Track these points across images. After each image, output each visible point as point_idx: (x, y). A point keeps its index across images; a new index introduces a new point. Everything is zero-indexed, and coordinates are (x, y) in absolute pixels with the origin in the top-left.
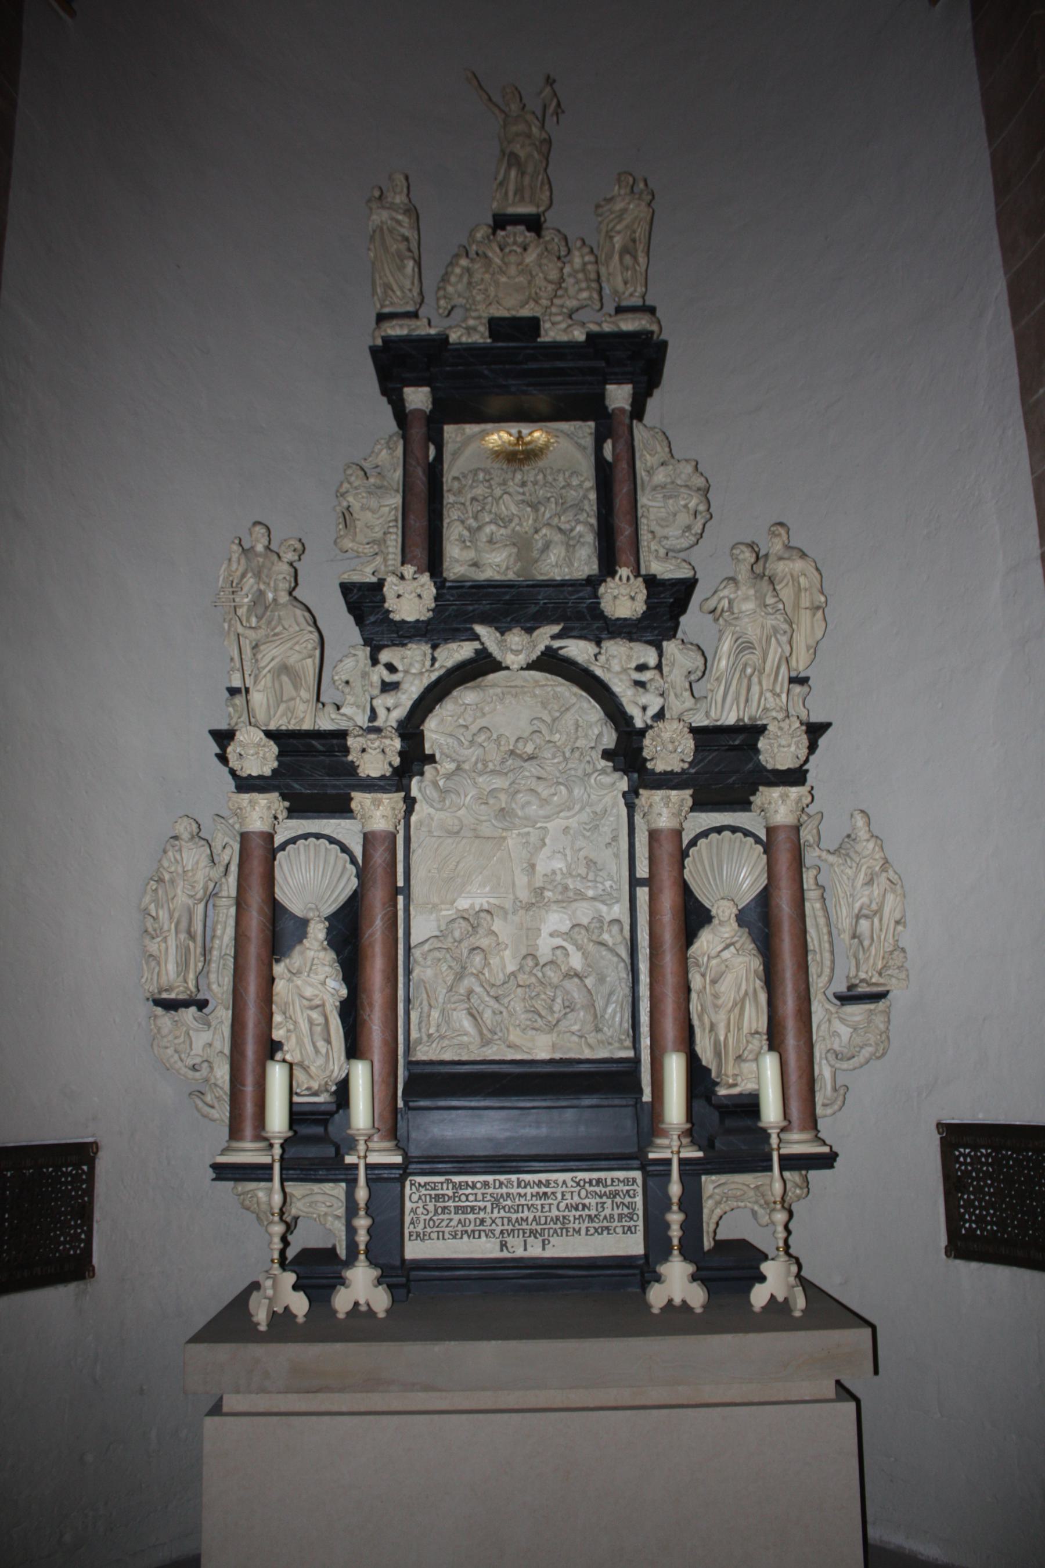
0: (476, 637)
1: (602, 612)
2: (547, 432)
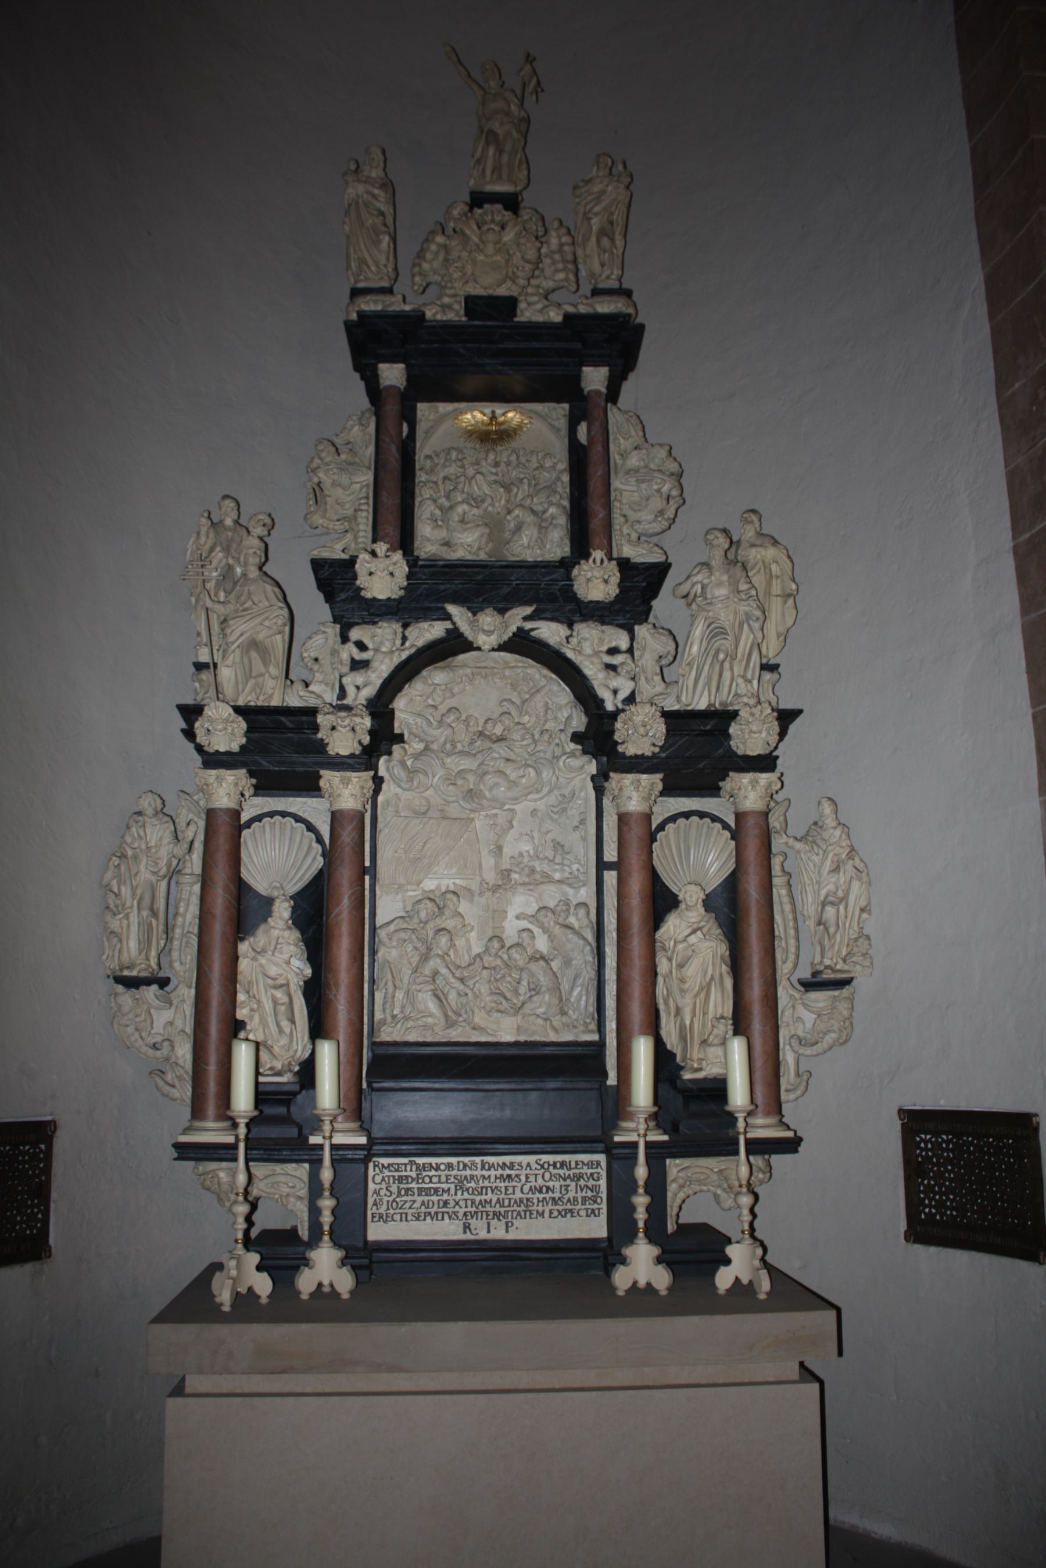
0: (448, 617)
1: (575, 594)
2: (521, 413)
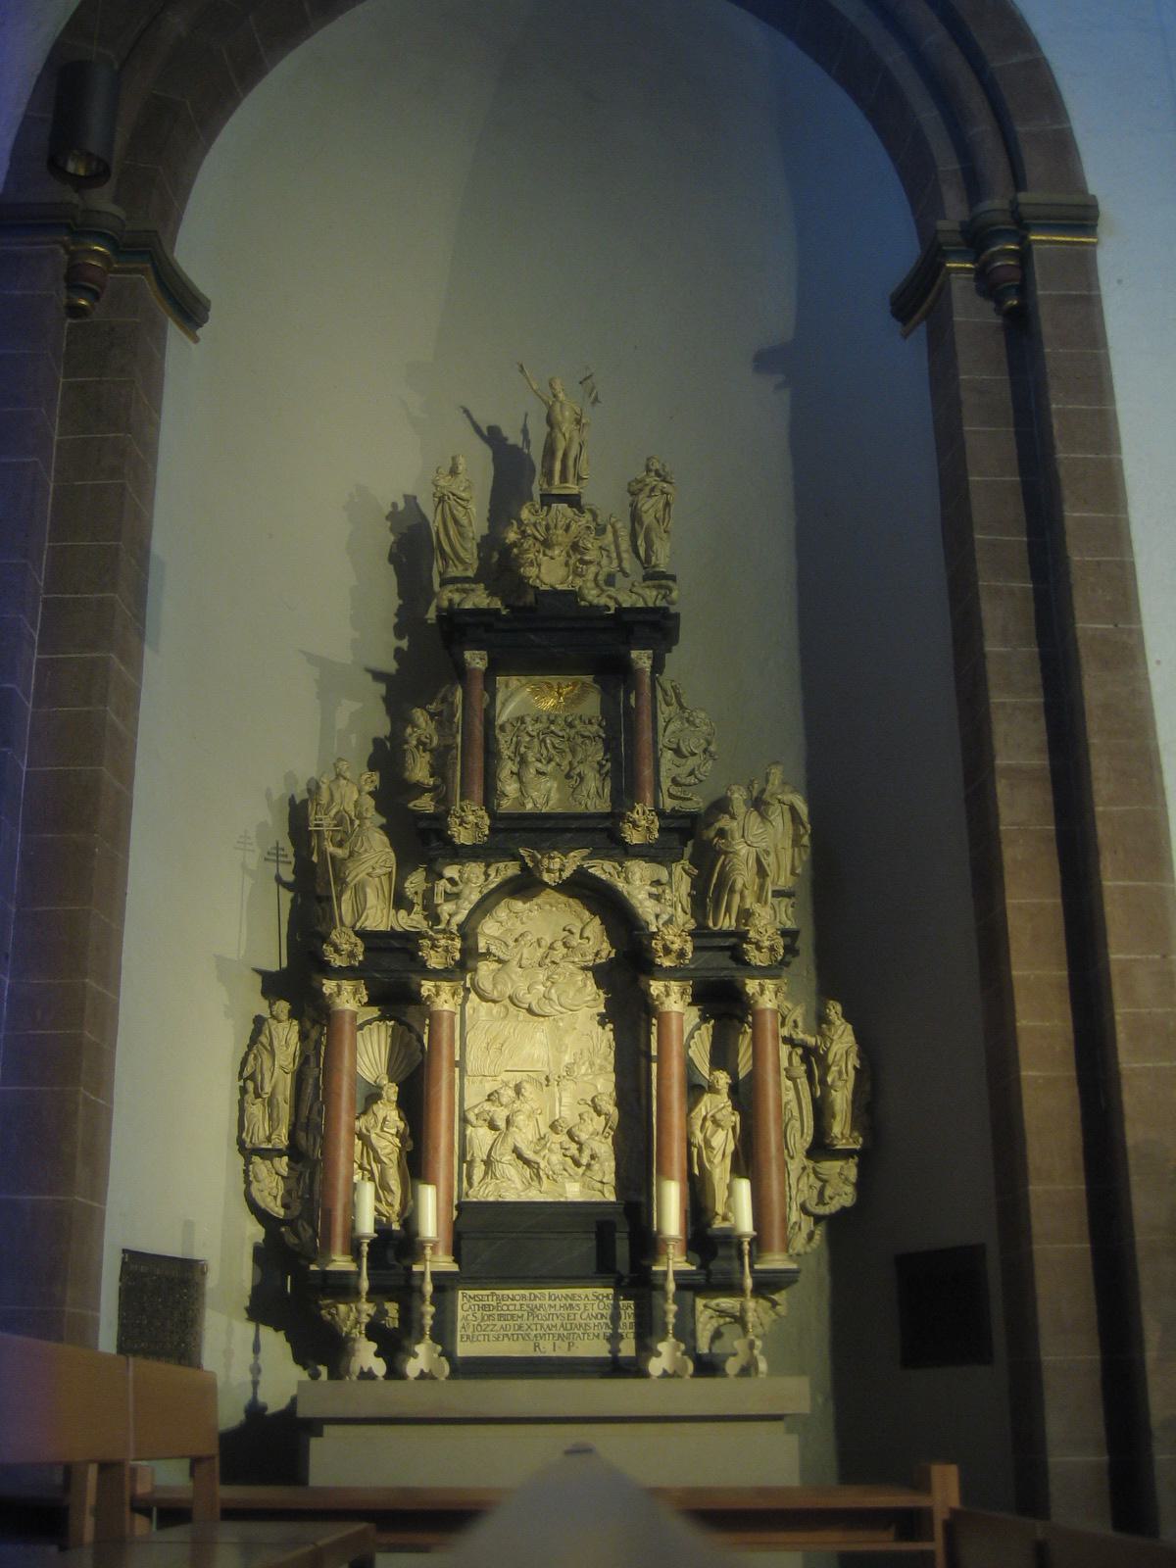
0: (522, 858)
